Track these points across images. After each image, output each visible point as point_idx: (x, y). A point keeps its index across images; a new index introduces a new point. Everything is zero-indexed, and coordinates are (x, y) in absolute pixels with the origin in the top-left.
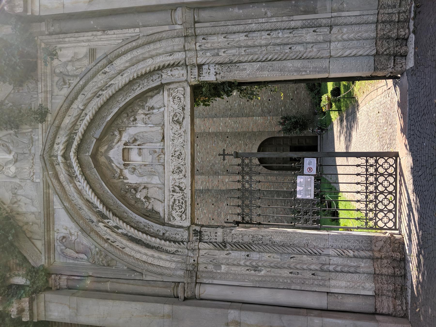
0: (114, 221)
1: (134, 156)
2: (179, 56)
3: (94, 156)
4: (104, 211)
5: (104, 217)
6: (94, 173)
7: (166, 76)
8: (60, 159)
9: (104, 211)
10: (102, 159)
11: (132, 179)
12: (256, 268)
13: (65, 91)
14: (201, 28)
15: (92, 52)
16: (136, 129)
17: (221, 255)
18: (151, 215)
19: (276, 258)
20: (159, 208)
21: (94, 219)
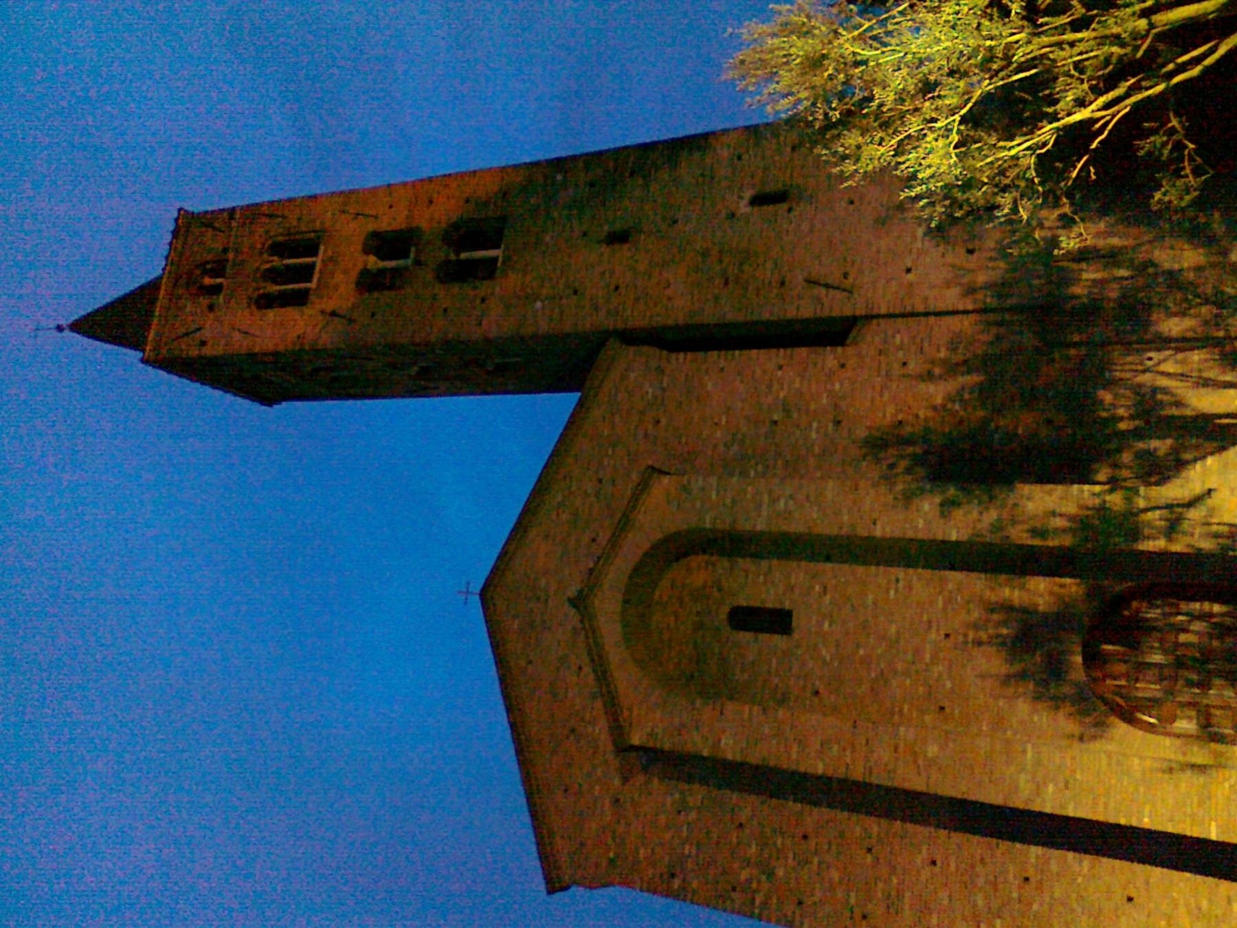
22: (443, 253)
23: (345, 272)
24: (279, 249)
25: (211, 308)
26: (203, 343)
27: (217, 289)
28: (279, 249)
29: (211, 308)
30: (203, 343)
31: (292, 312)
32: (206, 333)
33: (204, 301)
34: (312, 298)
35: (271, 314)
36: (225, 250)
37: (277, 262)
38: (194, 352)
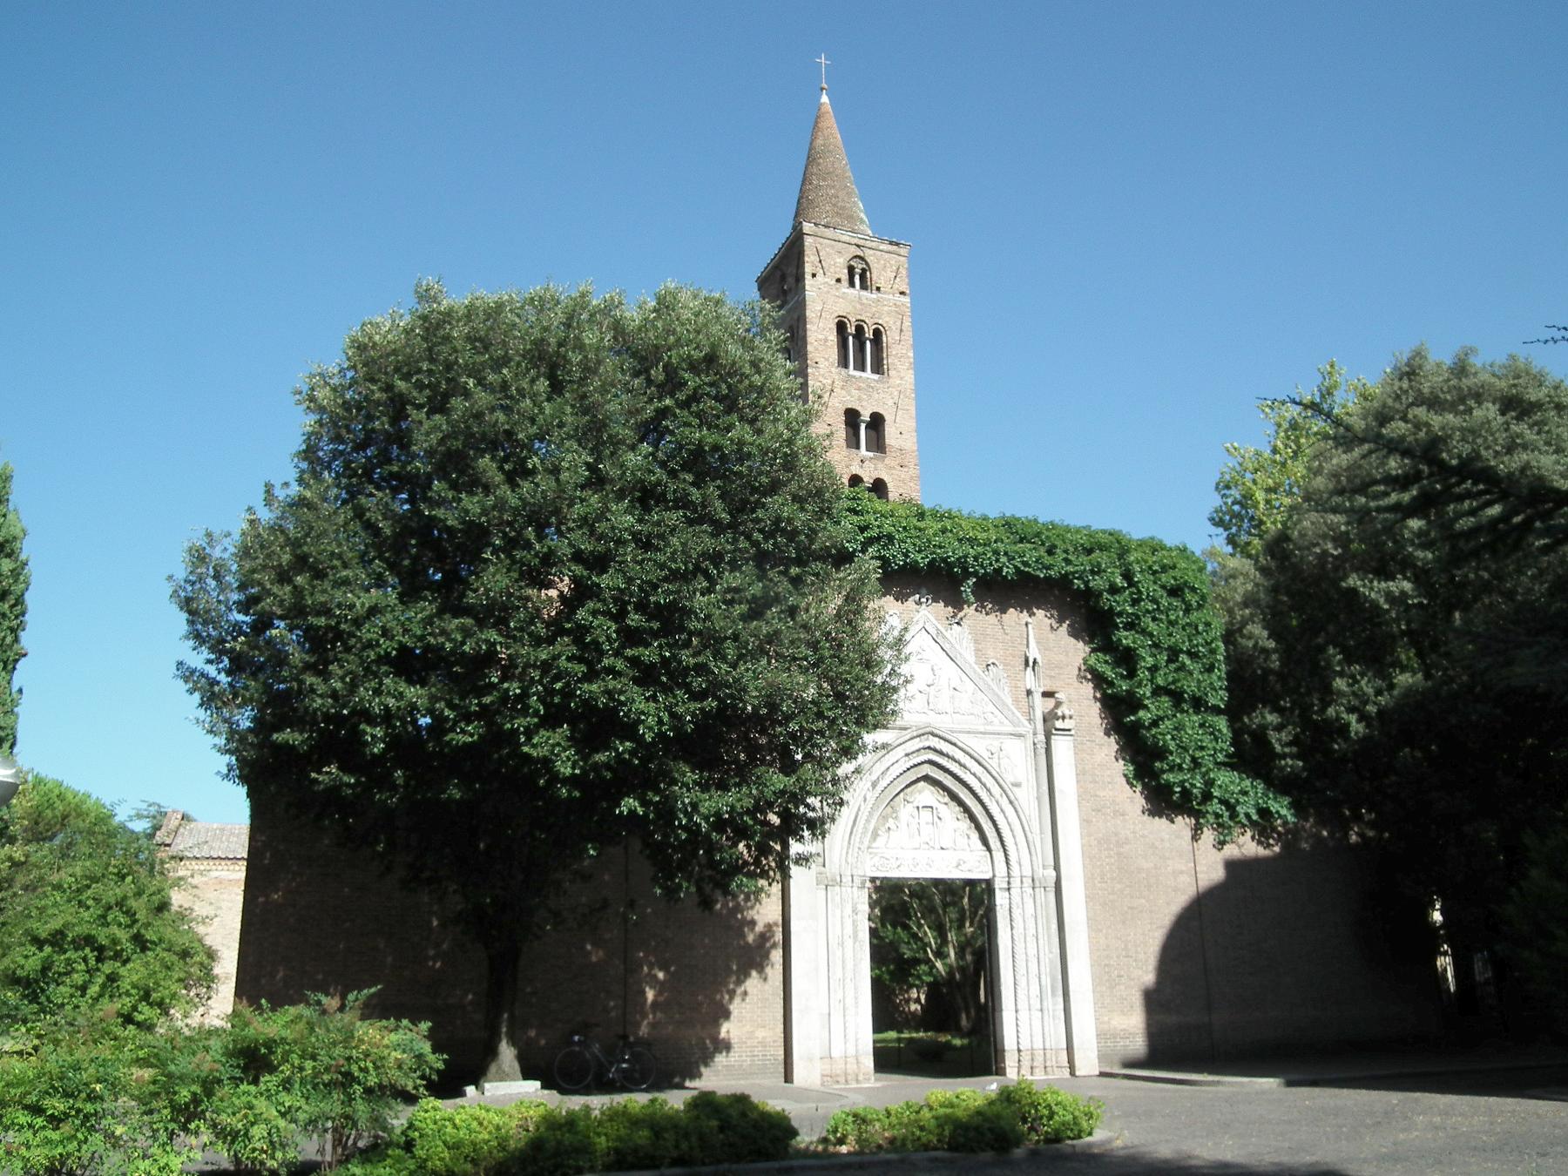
0: (871, 796)
1: (926, 814)
2: (1015, 871)
3: (926, 778)
4: (879, 788)
5: (874, 785)
6: (912, 776)
7: (999, 855)
8: (927, 744)
9: (879, 788)
10: (922, 784)
11: (906, 811)
12: (842, 944)
13: (986, 755)
14: (1039, 892)
15: (1017, 785)
16: (952, 820)
17: (848, 910)
18: (875, 835)
19: (850, 965)
20: (880, 841)
21: (874, 777)
22: (868, 480)
23: (860, 399)
24: (877, 333)
25: (838, 280)
26: (814, 275)
27: (852, 284)
28: (877, 333)
29: (838, 280)
30: (814, 275)
31: (833, 353)
32: (820, 277)
33: (844, 275)
34: (843, 371)
35: (833, 337)
36: (878, 289)
37: (869, 334)
38: (808, 269)
